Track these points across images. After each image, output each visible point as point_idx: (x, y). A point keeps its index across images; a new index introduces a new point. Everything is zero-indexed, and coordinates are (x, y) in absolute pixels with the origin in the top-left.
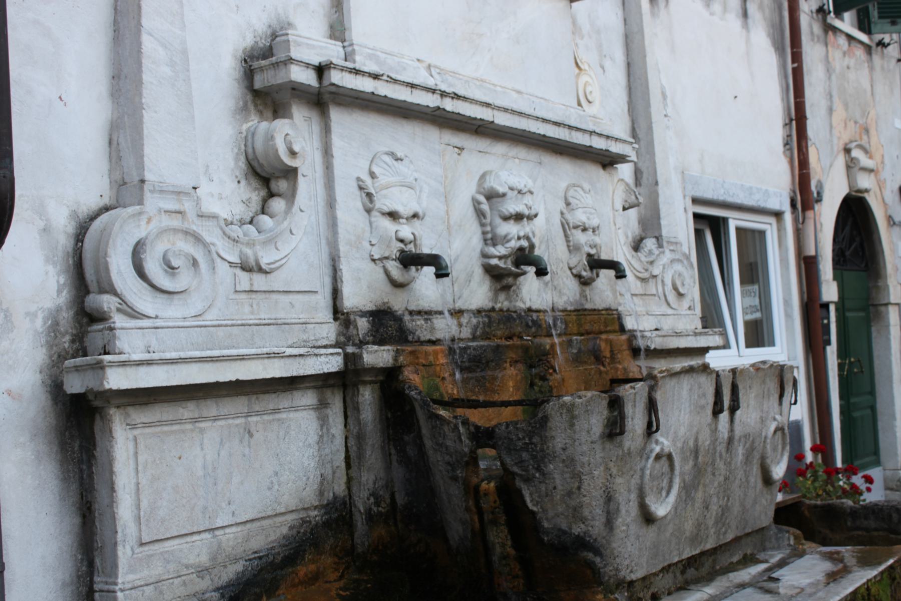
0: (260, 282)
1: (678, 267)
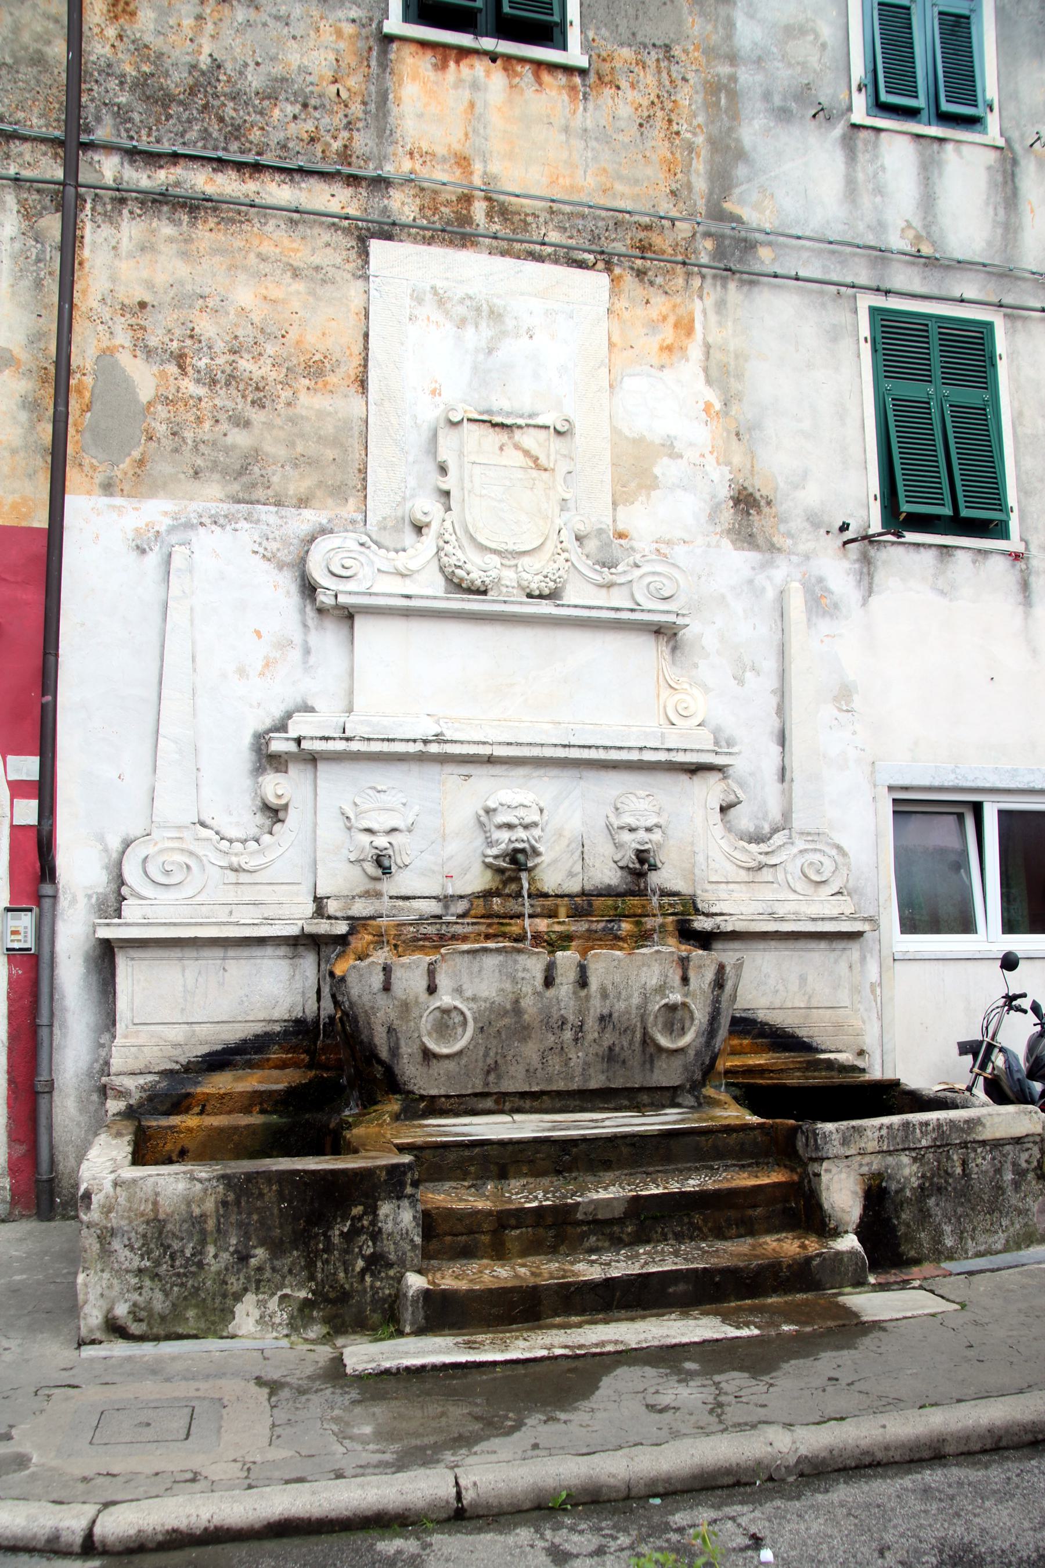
0: (244, 878)
1: (816, 857)
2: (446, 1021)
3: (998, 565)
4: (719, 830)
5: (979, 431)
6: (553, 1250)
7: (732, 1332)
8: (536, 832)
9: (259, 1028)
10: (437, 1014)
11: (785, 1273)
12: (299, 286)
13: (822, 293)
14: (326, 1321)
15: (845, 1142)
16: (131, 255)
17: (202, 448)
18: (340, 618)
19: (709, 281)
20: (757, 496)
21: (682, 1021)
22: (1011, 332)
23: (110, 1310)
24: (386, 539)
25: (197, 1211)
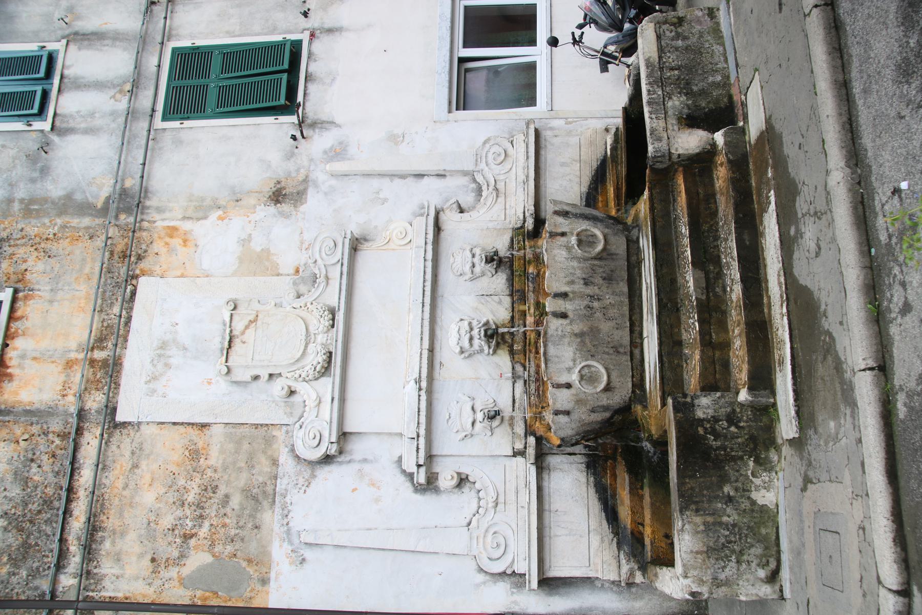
0: (501, 499)
1: (490, 156)
2: (587, 377)
3: (317, 46)
4: (474, 214)
5: (239, 57)
6: (724, 313)
7: (773, 206)
8: (475, 323)
9: (592, 491)
10: (583, 383)
11: (737, 175)
12: (144, 464)
13: (153, 150)
14: (767, 449)
15: (659, 139)
16: (122, 568)
17: (241, 524)
18: (345, 441)
19: (145, 217)
20: (274, 189)
21: (588, 236)
22: (179, 37)
23: (762, 580)
24: (297, 413)
25: (702, 528)
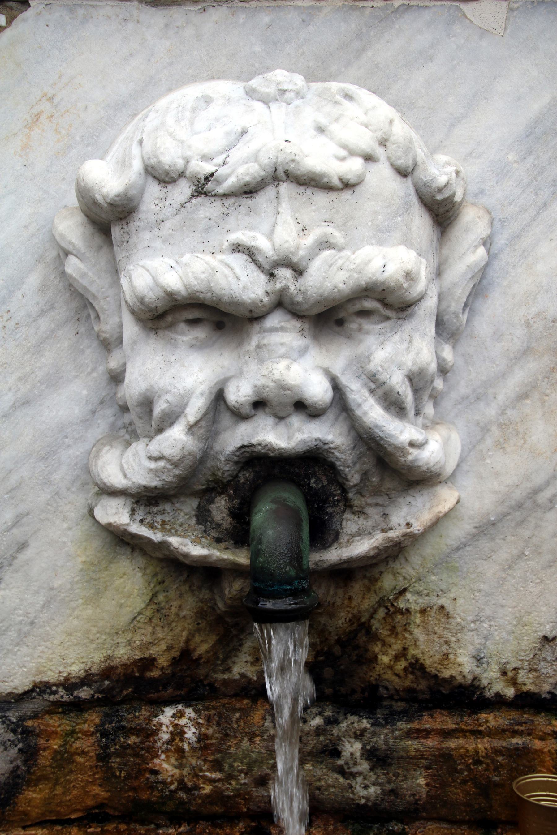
8: (398, 350)
